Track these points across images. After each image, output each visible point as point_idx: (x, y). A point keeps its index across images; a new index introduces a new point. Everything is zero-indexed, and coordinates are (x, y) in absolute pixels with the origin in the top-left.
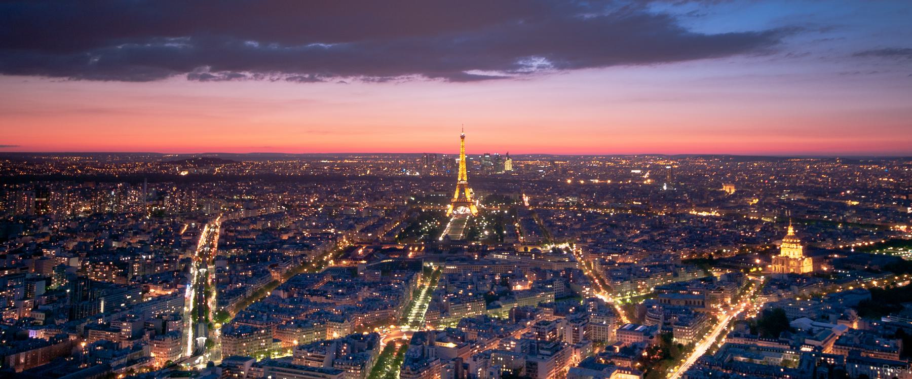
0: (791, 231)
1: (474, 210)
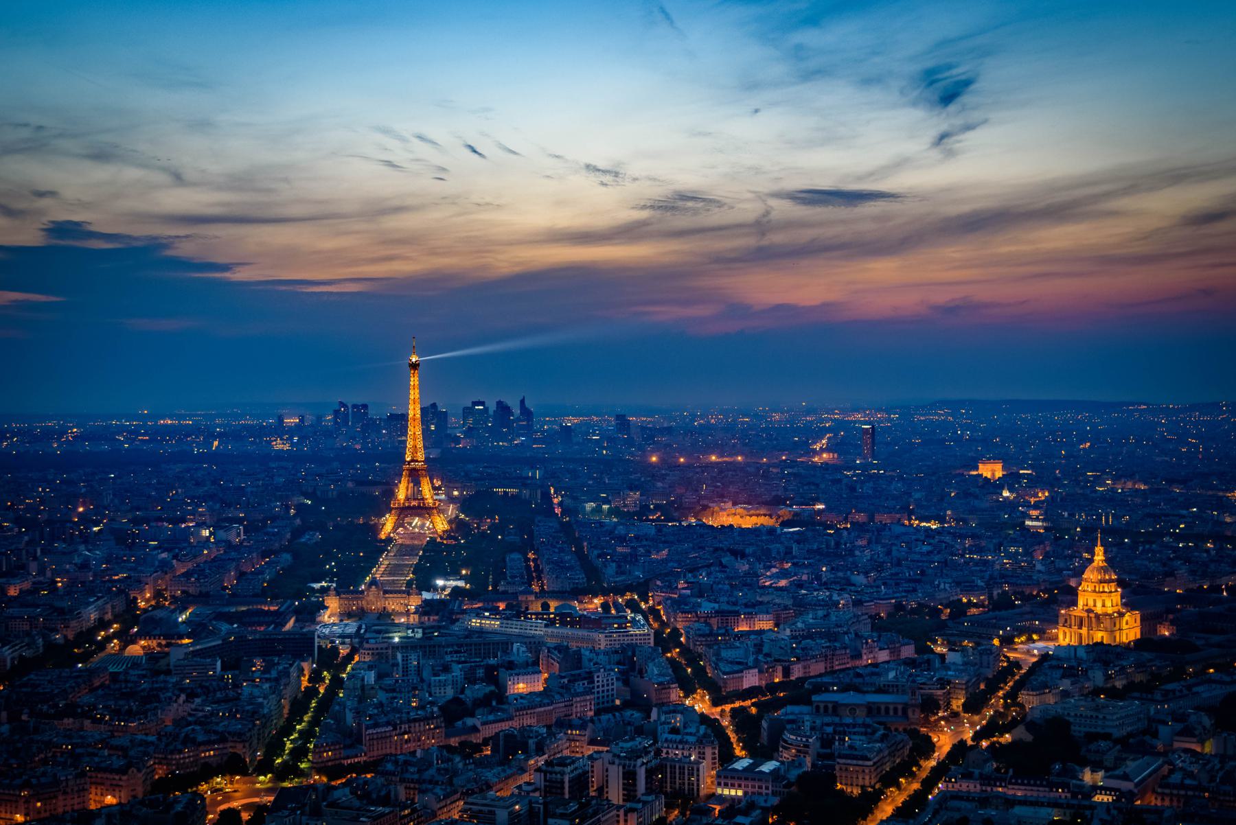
0: (1099, 556)
1: (441, 524)
